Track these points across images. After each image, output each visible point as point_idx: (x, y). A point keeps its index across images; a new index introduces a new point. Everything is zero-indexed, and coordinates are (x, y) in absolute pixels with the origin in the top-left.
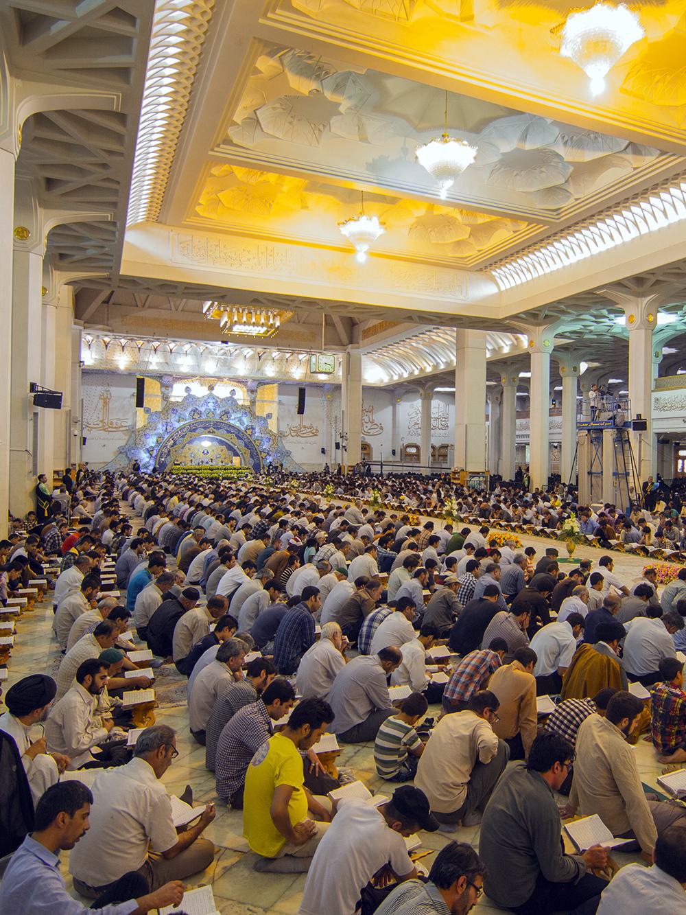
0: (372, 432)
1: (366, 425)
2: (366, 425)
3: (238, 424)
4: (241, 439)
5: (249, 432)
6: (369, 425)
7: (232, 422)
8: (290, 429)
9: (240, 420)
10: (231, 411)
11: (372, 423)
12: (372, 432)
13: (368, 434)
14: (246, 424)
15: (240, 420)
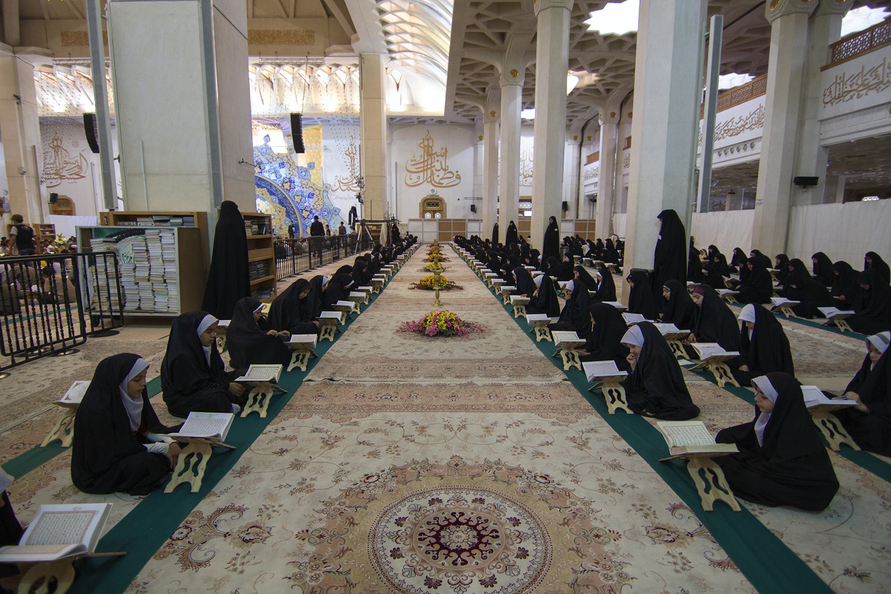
0: (445, 182)
1: (437, 173)
2: (437, 173)
3: (273, 177)
4: (274, 194)
5: (287, 186)
6: (441, 173)
7: (266, 175)
8: (339, 182)
9: (276, 172)
10: (265, 161)
11: (445, 170)
12: (445, 182)
13: (440, 185)
14: (284, 176)
15: (276, 172)
